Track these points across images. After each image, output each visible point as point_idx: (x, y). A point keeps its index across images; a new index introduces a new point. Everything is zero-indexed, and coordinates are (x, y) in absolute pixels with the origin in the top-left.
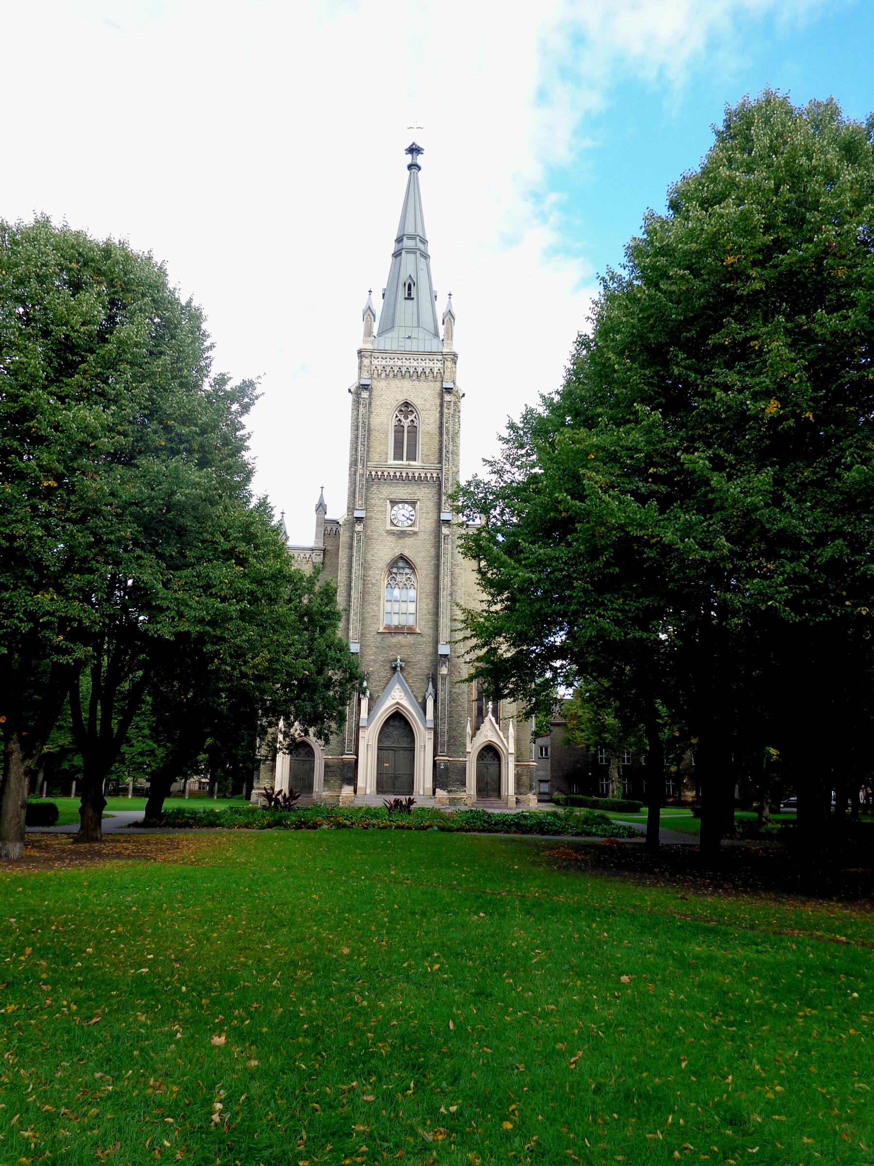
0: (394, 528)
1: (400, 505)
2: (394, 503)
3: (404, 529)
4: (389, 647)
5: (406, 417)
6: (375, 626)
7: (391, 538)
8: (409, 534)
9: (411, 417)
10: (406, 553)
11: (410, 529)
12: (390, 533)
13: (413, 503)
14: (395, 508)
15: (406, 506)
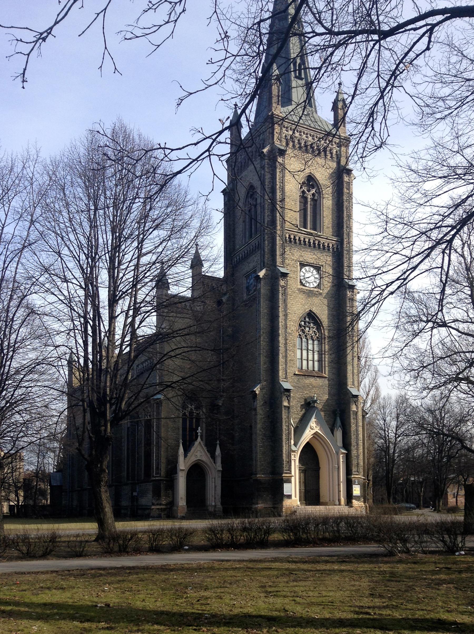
0: (304, 287)
1: (307, 268)
2: (303, 265)
3: (312, 289)
4: (304, 387)
5: (309, 191)
6: (293, 369)
7: (301, 296)
8: (315, 294)
9: (313, 191)
10: (314, 310)
11: (316, 290)
12: (300, 291)
13: (318, 268)
14: (303, 270)
15: (312, 269)
